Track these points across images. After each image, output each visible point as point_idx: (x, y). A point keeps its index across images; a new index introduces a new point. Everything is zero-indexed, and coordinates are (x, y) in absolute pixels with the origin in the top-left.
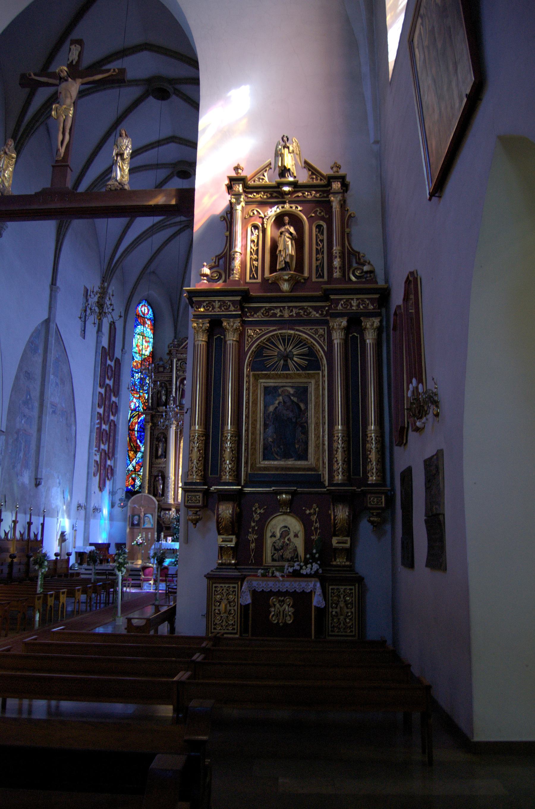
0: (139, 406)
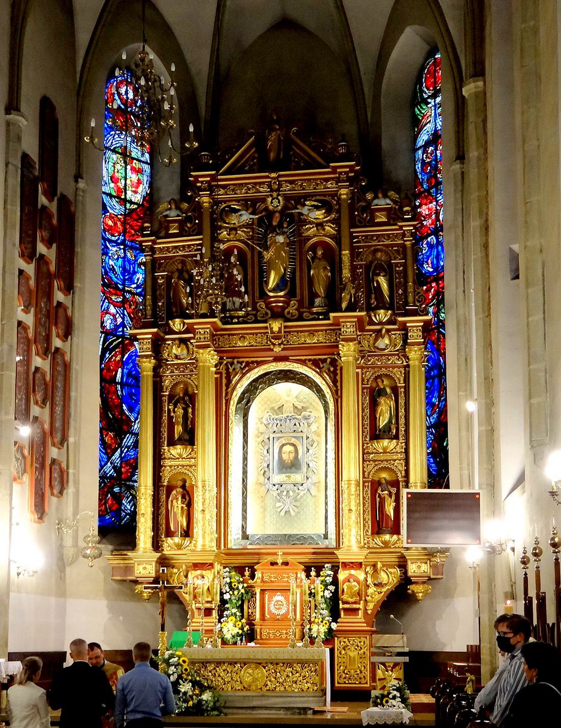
0: (123, 325)
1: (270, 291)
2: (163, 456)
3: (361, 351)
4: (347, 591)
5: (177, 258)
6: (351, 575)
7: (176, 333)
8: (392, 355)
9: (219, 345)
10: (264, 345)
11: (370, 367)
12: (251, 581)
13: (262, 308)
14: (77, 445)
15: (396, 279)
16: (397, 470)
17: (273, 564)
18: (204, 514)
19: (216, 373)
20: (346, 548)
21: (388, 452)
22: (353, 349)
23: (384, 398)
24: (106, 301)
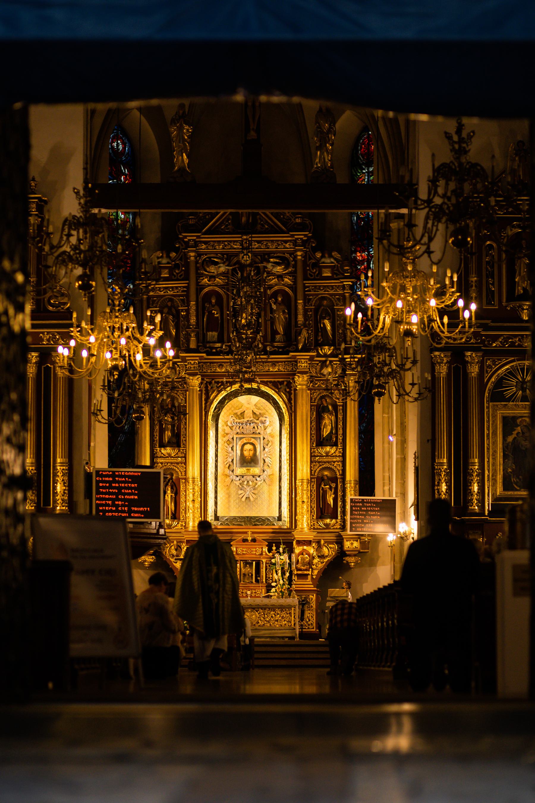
2: (156, 455)
21: (330, 456)
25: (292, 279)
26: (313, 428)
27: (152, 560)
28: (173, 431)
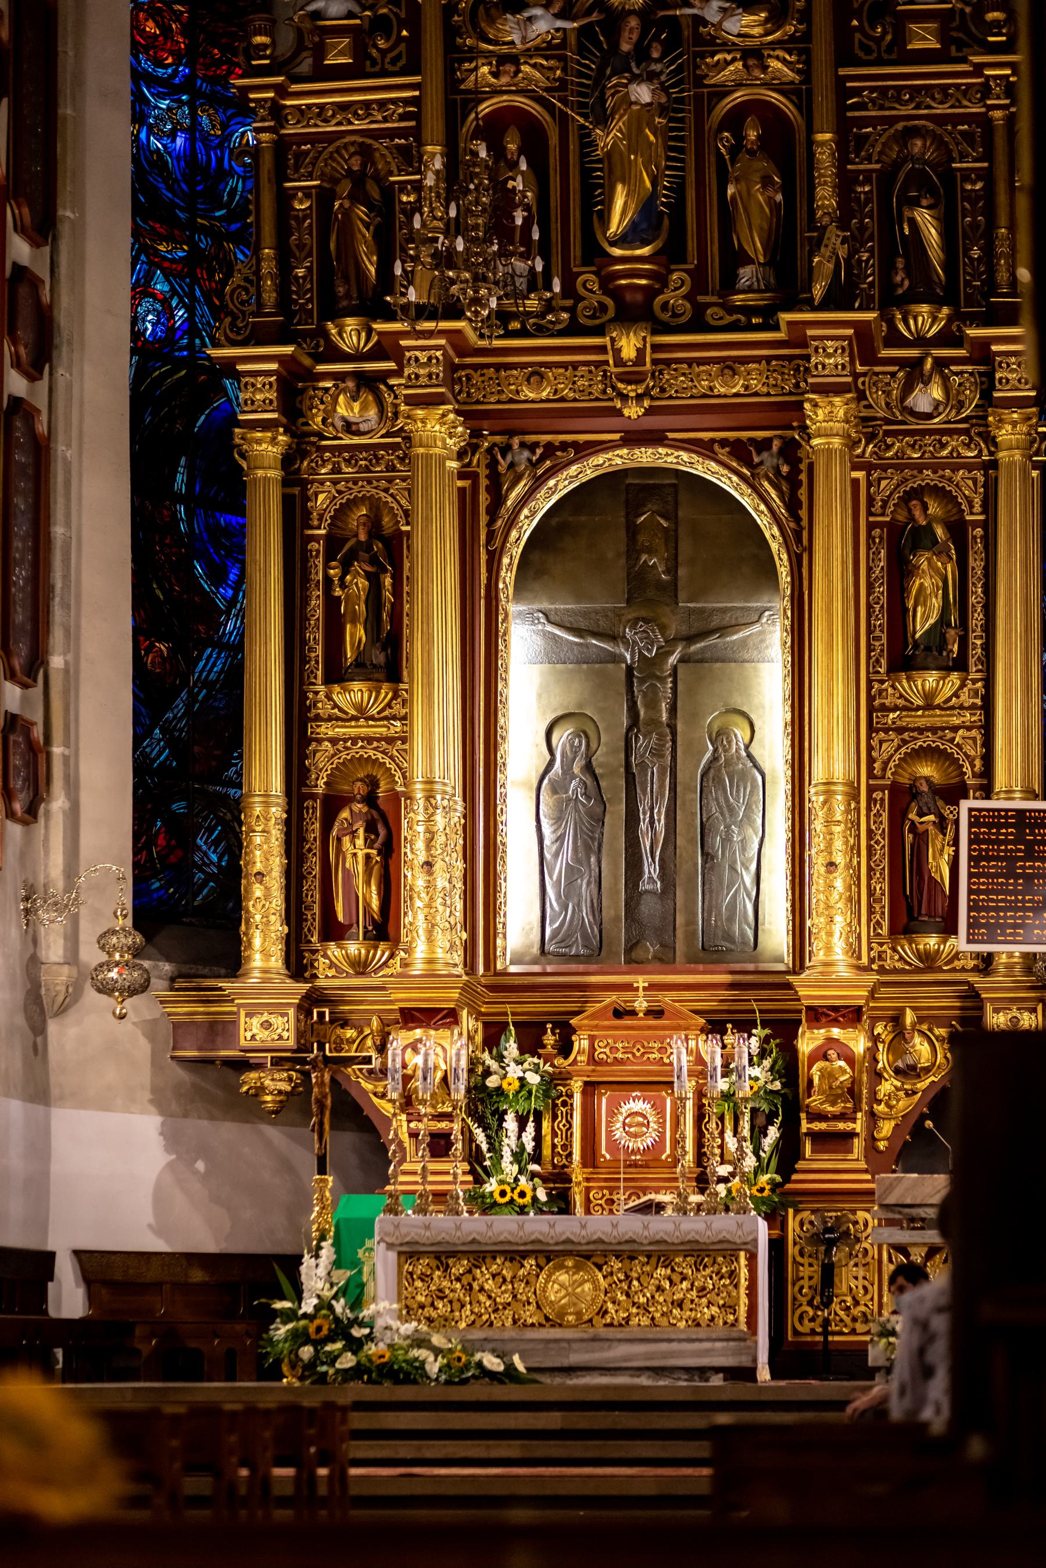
1: (613, 244)
2: (314, 712)
3: (865, 420)
4: (820, 1085)
5: (352, 138)
6: (830, 1041)
7: (346, 358)
8: (950, 432)
9: (469, 394)
10: (597, 399)
11: (890, 466)
12: (559, 1061)
13: (591, 291)
14: (71, 674)
15: (964, 217)
16: (961, 757)
17: (619, 1014)
18: (430, 873)
19: (462, 476)
20: (820, 969)
21: (939, 707)
22: (841, 413)
23: (927, 555)
24: (143, 257)
25: (798, 62)
26: (877, 607)
27: (285, 1087)
28: (373, 623)
